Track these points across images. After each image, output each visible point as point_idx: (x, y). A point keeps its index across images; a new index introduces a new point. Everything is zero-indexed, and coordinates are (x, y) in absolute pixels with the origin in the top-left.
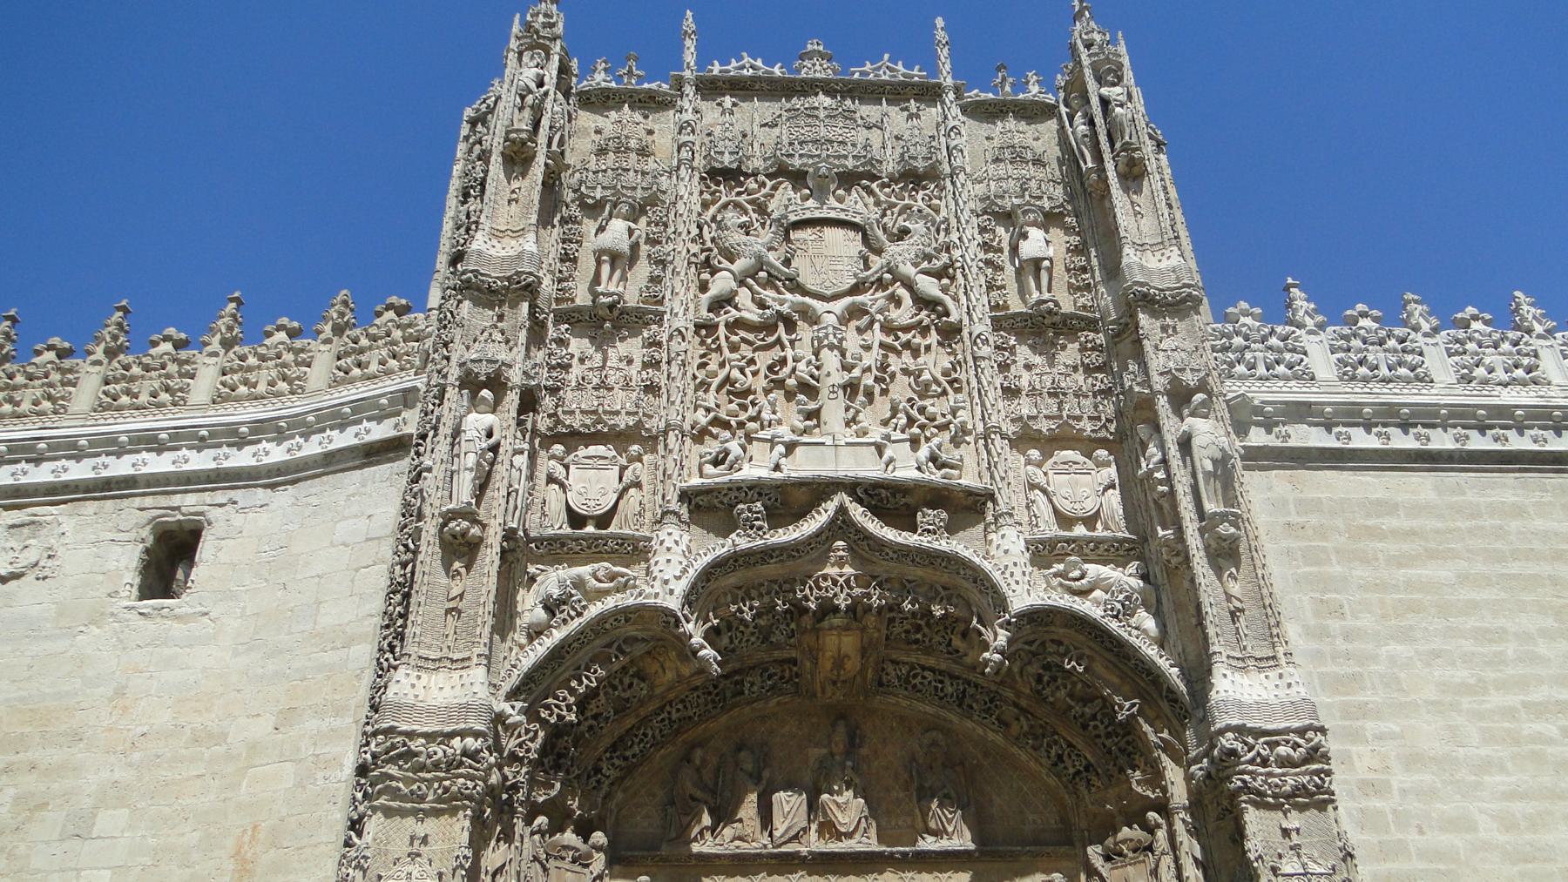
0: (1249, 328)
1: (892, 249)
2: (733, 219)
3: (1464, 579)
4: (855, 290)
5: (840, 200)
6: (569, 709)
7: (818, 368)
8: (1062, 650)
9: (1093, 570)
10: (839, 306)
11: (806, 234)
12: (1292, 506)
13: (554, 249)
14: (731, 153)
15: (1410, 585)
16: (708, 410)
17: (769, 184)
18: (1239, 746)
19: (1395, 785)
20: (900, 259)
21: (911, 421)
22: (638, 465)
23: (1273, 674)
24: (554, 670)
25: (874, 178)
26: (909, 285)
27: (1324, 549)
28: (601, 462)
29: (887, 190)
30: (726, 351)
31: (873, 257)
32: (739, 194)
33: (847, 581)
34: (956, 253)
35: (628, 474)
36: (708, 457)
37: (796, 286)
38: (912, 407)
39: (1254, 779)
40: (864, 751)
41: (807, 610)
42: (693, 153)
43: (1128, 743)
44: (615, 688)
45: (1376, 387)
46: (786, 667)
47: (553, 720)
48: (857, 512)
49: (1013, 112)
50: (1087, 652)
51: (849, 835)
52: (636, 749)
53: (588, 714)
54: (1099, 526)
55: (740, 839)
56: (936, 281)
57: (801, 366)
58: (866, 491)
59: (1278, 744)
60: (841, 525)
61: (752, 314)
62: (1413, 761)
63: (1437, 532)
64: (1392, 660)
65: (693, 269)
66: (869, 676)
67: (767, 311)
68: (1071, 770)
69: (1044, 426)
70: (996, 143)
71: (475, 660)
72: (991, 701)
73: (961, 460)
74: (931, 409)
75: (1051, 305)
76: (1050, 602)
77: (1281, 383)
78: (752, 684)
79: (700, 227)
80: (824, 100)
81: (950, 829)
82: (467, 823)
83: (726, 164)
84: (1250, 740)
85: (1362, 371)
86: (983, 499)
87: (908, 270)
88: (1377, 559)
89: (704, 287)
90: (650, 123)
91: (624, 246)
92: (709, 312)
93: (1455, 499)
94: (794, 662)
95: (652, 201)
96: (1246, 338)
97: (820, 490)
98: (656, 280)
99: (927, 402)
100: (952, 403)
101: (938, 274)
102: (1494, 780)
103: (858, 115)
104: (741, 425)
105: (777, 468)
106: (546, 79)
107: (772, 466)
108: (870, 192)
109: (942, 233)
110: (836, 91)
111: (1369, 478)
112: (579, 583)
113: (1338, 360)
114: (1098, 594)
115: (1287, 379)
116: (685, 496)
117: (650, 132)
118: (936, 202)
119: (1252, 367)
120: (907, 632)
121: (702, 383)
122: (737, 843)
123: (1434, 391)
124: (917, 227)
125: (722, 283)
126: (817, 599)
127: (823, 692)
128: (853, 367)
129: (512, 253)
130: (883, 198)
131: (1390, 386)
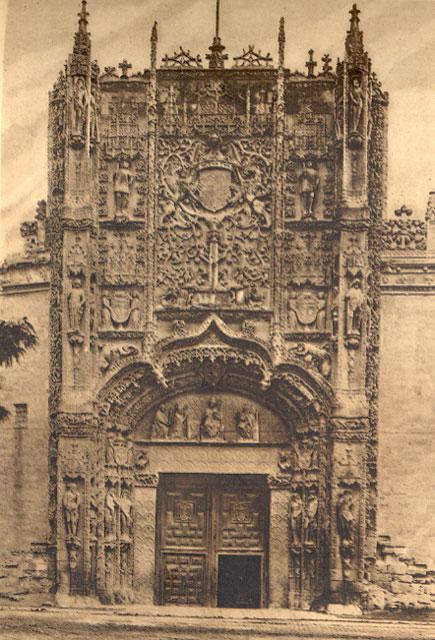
17: (191, 142)
26: (251, 205)
35: (133, 304)
48: (219, 322)
51: (214, 437)
56: (263, 204)
57: (202, 251)
60: (213, 327)
61: (182, 223)
74: (254, 273)
87: (250, 197)
92: (164, 221)
96: (400, 227)
98: (140, 203)
116: (156, 313)
118: (268, 153)
119: (399, 243)
125: (170, 208)
128: (223, 251)
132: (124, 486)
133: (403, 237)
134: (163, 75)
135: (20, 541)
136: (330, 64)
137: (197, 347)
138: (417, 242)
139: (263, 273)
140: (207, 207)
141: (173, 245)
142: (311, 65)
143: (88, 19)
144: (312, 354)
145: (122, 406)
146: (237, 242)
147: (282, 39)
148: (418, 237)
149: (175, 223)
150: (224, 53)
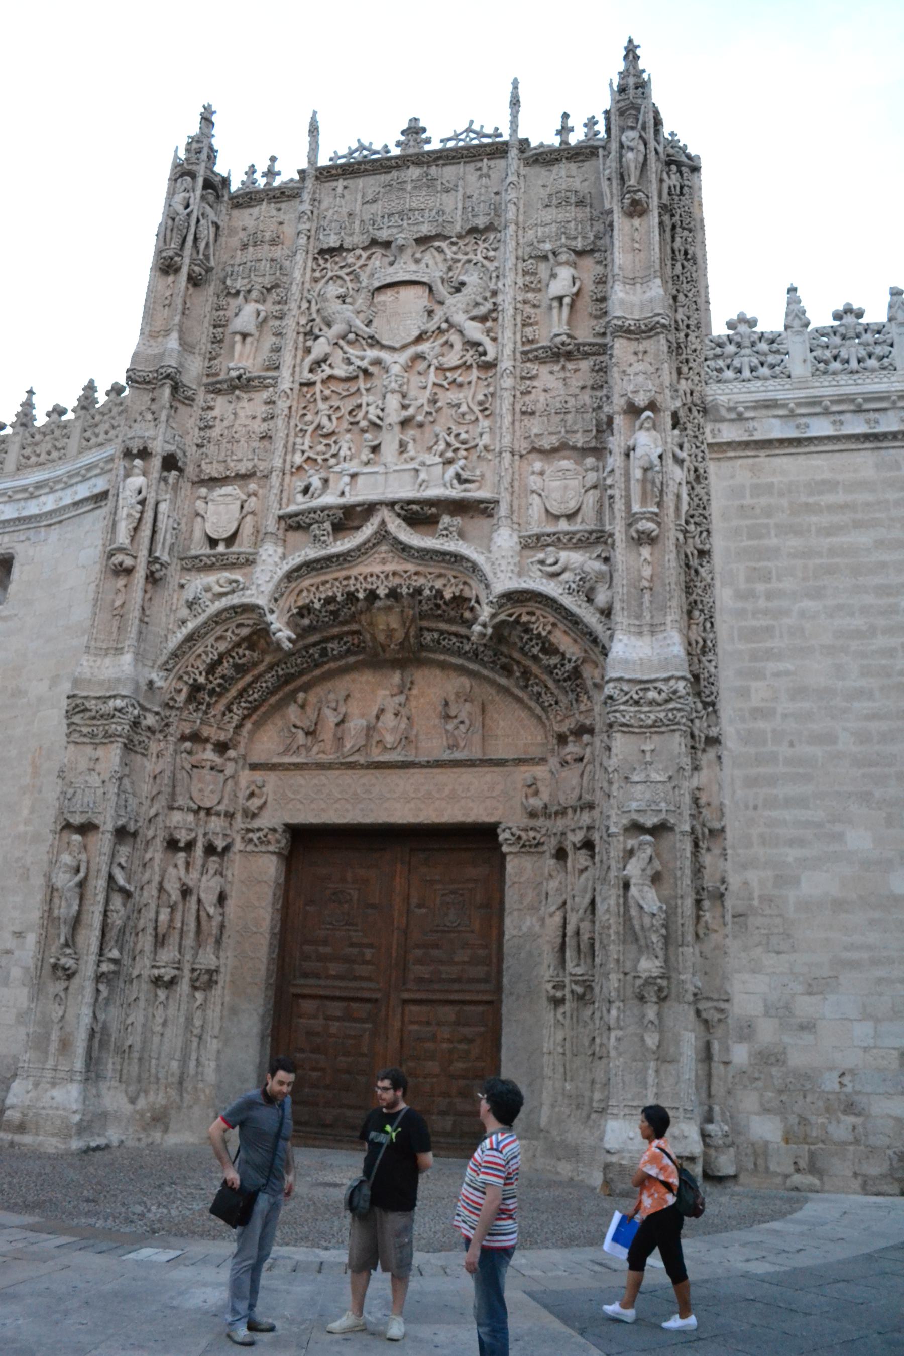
0: (742, 337)
1: (450, 300)
2: (333, 290)
3: (880, 544)
4: (419, 339)
5: (417, 261)
6: (201, 673)
7: (382, 410)
8: (534, 619)
9: (564, 556)
10: (403, 357)
11: (386, 297)
12: (748, 492)
13: (205, 336)
14: (336, 234)
15: (832, 552)
16: (303, 452)
17: (365, 255)
18: (616, 693)
19: (780, 710)
20: (453, 309)
21: (448, 445)
22: (253, 499)
23: (660, 636)
24: (190, 648)
25: (446, 238)
27: (767, 526)
28: (230, 498)
29: (454, 248)
30: (320, 402)
31: (436, 307)
32: (341, 267)
33: (387, 576)
34: (499, 299)
35: (246, 505)
36: (299, 489)
37: (374, 342)
38: (449, 435)
39: (624, 716)
40: (415, 692)
41: (357, 599)
42: (309, 237)
43: (577, 685)
44: (233, 658)
45: (843, 379)
46: (355, 637)
47: (191, 681)
49: (567, 158)
50: (552, 620)
52: (256, 696)
53: (217, 675)
54: (579, 519)
55: (324, 752)
56: (479, 325)
57: (372, 409)
58: (402, 508)
59: (648, 689)
60: (383, 535)
62: (799, 692)
63: (868, 504)
64: (802, 614)
65: (301, 338)
66: (412, 640)
67: (351, 368)
68: (547, 704)
69: (547, 443)
70: (548, 190)
71: (126, 649)
72: (495, 655)
73: (482, 476)
74: (463, 436)
75: (564, 338)
76: (524, 586)
77: (759, 383)
78: (333, 650)
79: (309, 302)
80: (414, 172)
81: (462, 744)
82: (118, 751)
83: (332, 245)
84: (626, 688)
85: (836, 365)
86: (492, 506)
87: (459, 318)
88: (809, 531)
89: (308, 350)
90: (282, 217)
91: (251, 328)
93: (889, 474)
94: (357, 632)
95: (276, 286)
96: (739, 345)
97: (370, 509)
99: (462, 430)
100: (479, 430)
101: (483, 319)
102: (863, 706)
103: (439, 182)
104: (326, 460)
105: (343, 494)
106: (192, 201)
107: (339, 493)
108: (440, 250)
109: (494, 280)
110: (423, 163)
111: (818, 461)
112: (208, 589)
113: (815, 358)
114: (566, 576)
115: (766, 379)
117: (281, 223)
118: (492, 253)
119: (740, 371)
120: (431, 609)
121: (301, 430)
122: (321, 756)
123: (893, 379)
124: (472, 278)
125: (320, 348)
126: (365, 590)
127: (384, 651)
129: (156, 351)
130: (450, 255)
131: (856, 376)
132: (210, 850)
133: (746, 359)
134: (326, 175)
135: (196, 974)
136: (596, 128)
137: (354, 572)
138: (772, 366)
139: (481, 435)
140: (384, 342)
141: (322, 406)
142: (564, 130)
143: (214, 118)
144: (573, 570)
145: (212, 692)
146: (437, 390)
147: (515, 103)
148: (771, 359)
149: (328, 371)
150: (424, 136)
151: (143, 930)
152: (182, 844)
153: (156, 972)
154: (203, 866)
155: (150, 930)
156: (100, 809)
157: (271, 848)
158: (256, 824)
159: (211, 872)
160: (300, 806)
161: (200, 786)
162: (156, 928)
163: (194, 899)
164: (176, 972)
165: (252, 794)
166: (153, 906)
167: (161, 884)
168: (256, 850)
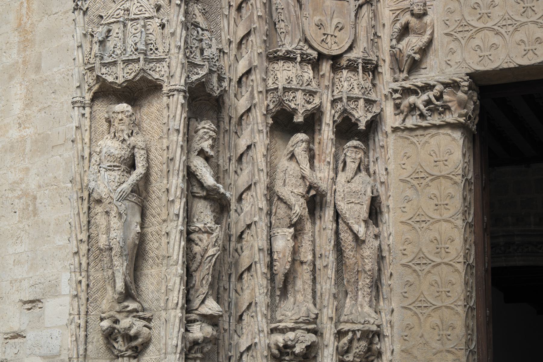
151: (249, 269)
152: (299, 119)
153: (280, 339)
154: (336, 157)
155: (261, 268)
156: (160, 54)
157: (449, 118)
158: (419, 79)
159: (352, 166)
160: (496, 40)
161: (316, 19)
162: (271, 266)
163: (329, 213)
164: (311, 338)
165: (405, 30)
166: (262, 225)
167: (270, 188)
168: (424, 124)
